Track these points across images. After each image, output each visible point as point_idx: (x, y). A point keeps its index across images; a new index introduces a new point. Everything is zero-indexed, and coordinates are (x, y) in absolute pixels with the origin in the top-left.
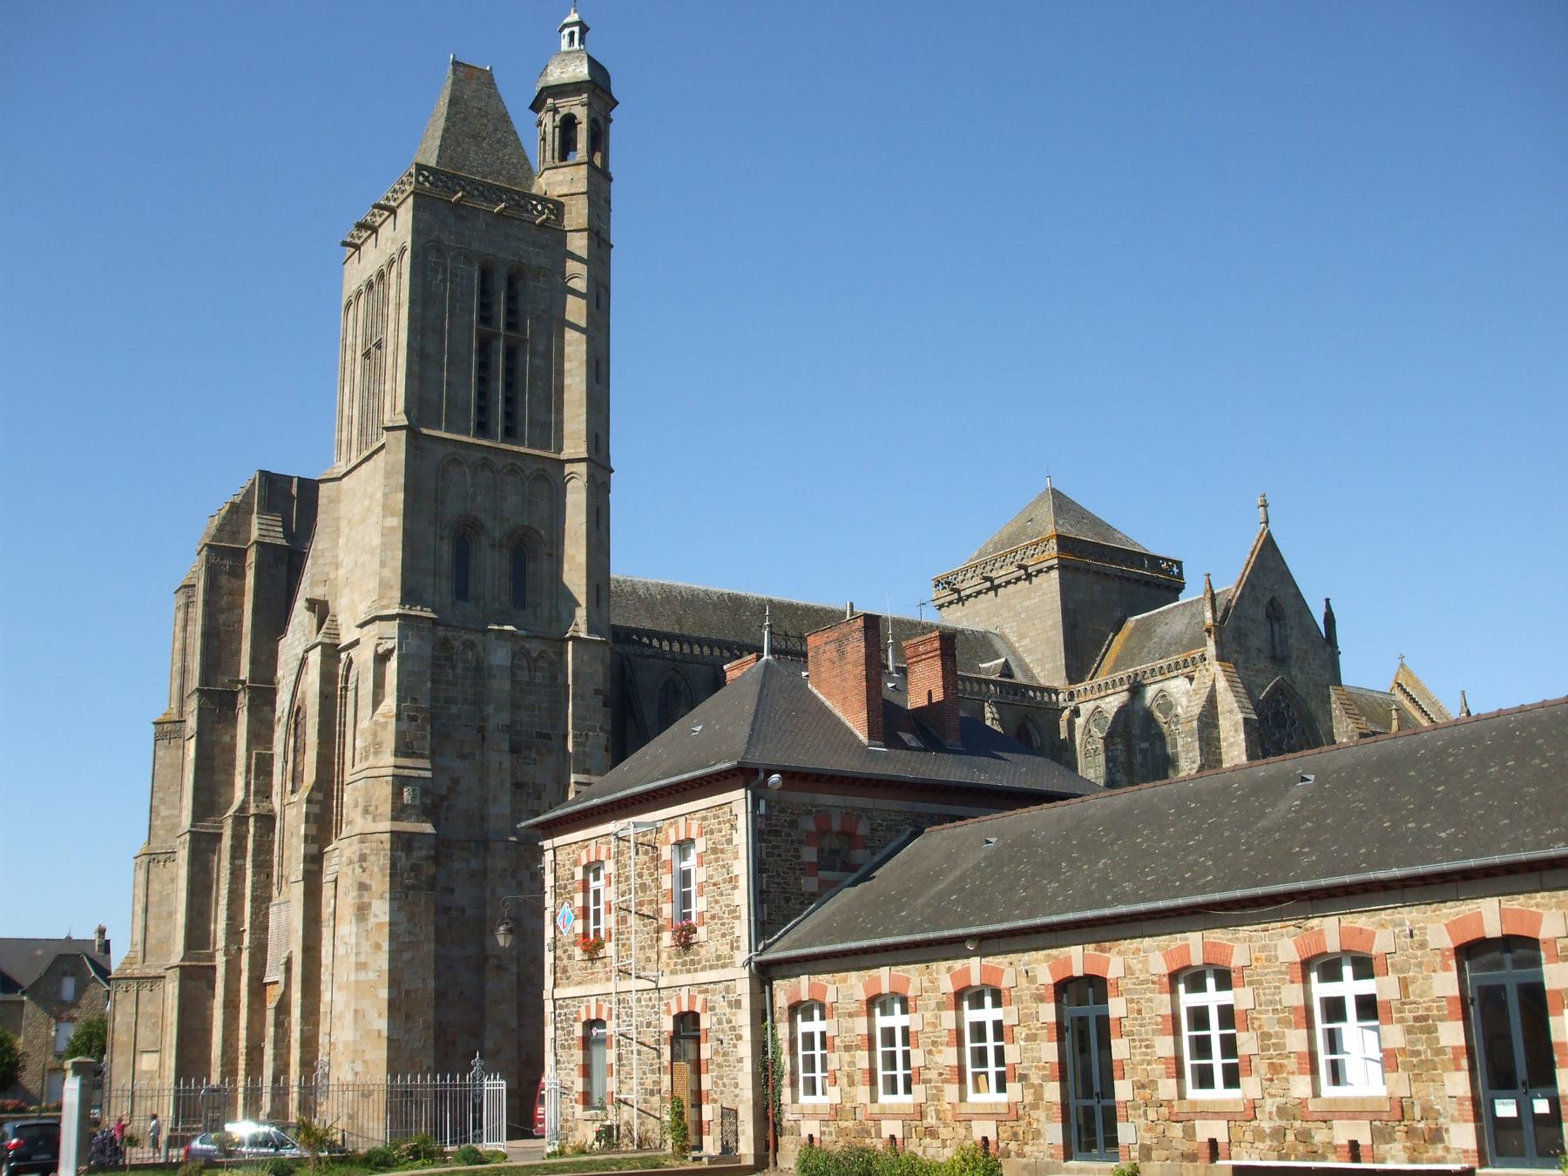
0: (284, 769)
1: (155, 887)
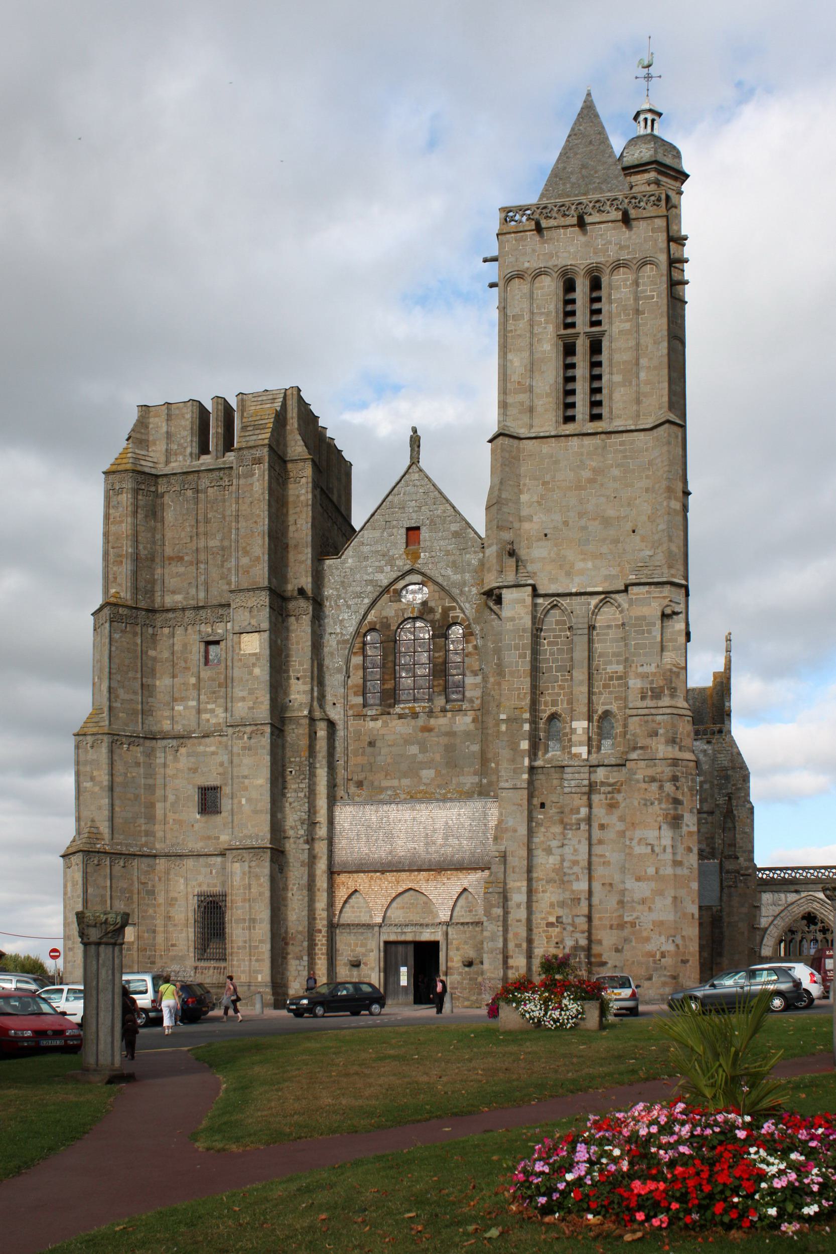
0: (345, 684)
1: (119, 767)
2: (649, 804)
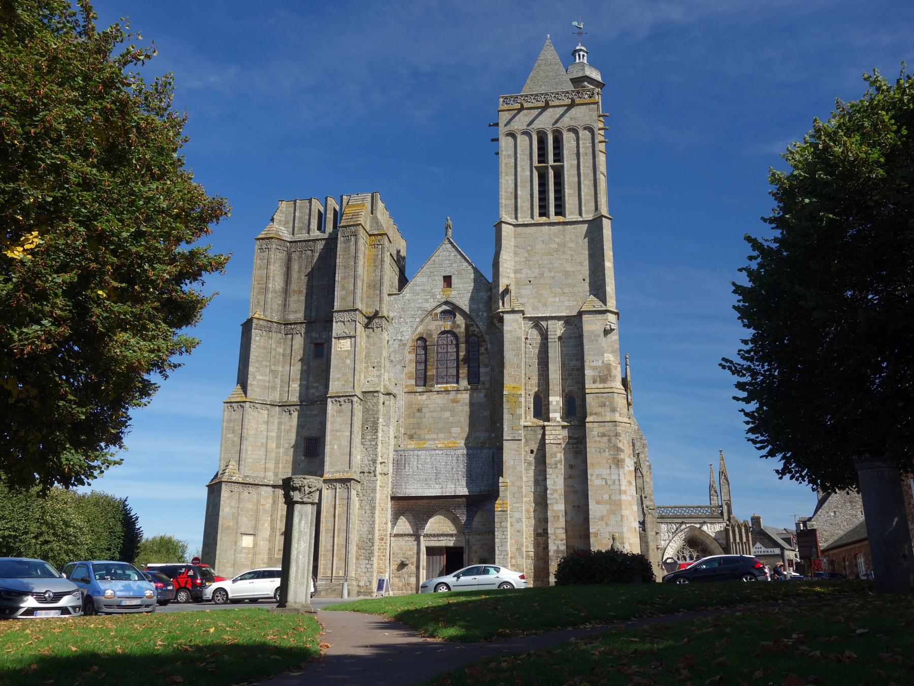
2: (602, 451)
